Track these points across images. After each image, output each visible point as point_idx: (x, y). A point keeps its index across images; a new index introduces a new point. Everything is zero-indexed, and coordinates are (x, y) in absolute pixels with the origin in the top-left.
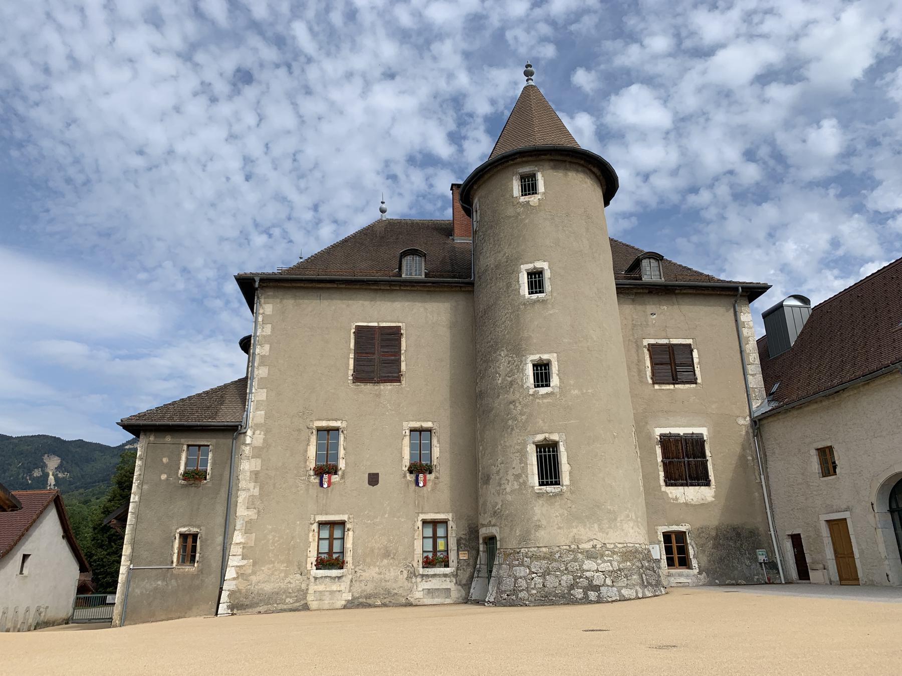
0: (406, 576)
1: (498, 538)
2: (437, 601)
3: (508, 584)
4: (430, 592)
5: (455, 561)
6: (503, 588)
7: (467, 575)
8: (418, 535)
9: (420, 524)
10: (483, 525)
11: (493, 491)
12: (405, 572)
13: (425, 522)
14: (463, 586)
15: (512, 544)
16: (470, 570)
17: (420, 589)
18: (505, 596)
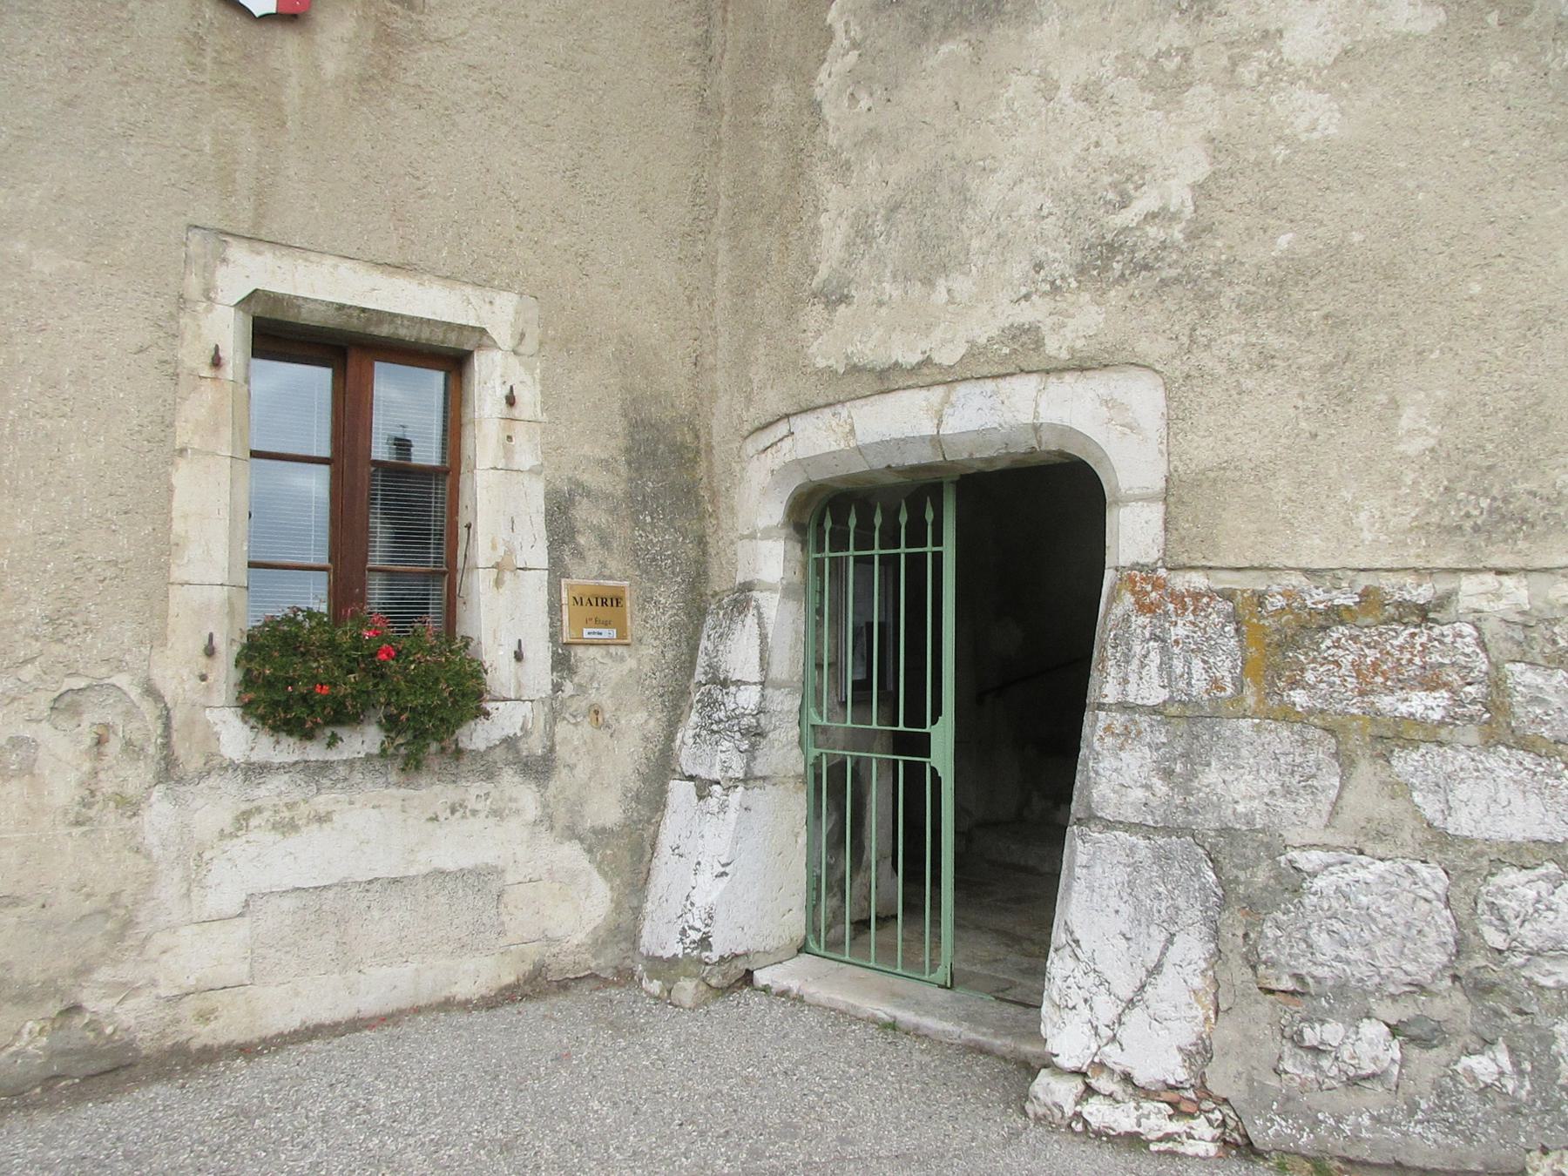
0: (63, 790)
1: (1132, 468)
2: (378, 988)
3: (1369, 911)
4: (325, 908)
5: (540, 654)
6: (1325, 957)
7: (626, 754)
8: (198, 410)
9: (227, 329)
10: (885, 380)
11: (1071, 71)
12: (62, 749)
13: (278, 334)
14: (596, 841)
15: (1347, 531)
16: (639, 722)
17: (224, 895)
18: (1371, 1044)
